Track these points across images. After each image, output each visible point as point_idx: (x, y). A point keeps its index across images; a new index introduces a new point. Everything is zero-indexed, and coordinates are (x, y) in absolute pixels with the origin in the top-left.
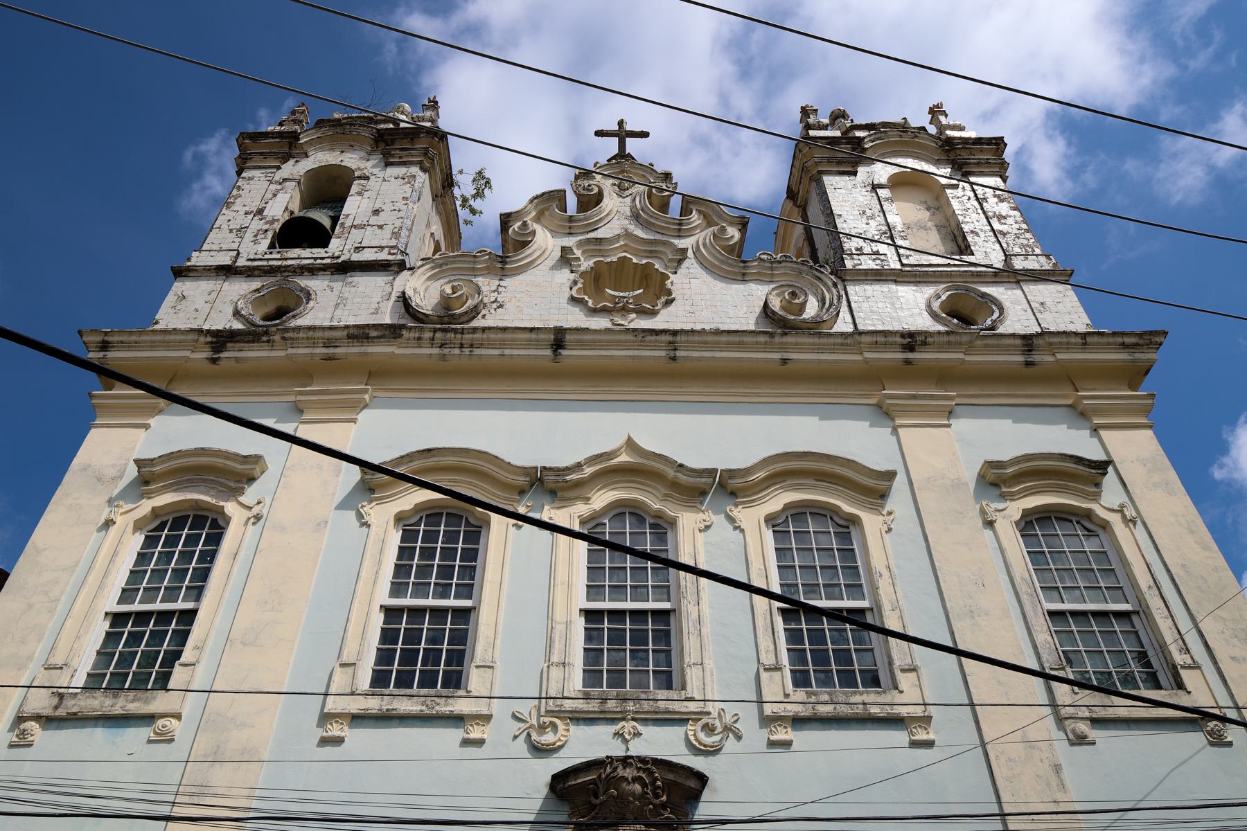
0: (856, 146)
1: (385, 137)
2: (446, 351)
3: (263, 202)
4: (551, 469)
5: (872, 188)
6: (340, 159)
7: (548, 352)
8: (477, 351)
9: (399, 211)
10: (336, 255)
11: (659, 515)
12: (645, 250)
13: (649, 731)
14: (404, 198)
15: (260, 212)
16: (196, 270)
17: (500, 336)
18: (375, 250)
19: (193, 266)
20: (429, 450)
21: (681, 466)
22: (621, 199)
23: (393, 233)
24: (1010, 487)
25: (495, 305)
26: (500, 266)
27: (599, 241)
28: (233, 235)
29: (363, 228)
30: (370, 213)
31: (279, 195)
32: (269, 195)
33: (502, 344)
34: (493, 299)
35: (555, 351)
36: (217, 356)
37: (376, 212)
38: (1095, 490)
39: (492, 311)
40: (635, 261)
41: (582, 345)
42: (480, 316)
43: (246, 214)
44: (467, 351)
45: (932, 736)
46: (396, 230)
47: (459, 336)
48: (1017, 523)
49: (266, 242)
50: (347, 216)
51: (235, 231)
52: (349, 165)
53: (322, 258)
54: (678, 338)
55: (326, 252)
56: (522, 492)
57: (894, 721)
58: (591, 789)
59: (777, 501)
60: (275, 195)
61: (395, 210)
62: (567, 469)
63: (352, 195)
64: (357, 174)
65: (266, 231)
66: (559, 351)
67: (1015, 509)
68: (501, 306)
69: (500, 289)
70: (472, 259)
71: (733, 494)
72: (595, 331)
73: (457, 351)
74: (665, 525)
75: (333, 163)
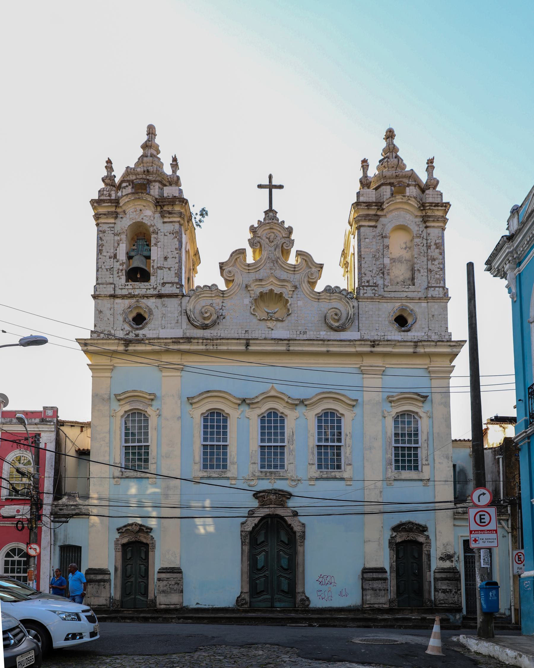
0: (379, 208)
1: (160, 204)
2: (208, 347)
3: (115, 249)
4: (248, 399)
5: (382, 237)
6: (141, 217)
7: (243, 348)
8: (219, 348)
9: (175, 258)
10: (155, 287)
11: (282, 413)
12: (280, 285)
13: (278, 482)
14: (176, 248)
15: (115, 256)
16: (101, 297)
17: (226, 341)
18: (170, 285)
19: (100, 294)
20: (208, 391)
21: (289, 397)
22: (270, 249)
23: (176, 273)
24: (395, 403)
25: (222, 317)
26: (222, 295)
27: (261, 280)
28: (108, 273)
29: (162, 269)
30: (163, 259)
31: (121, 245)
32: (116, 245)
33: (227, 344)
34: (221, 314)
35: (246, 347)
36: (126, 349)
37: (166, 258)
38: (422, 405)
39: (221, 321)
40: (275, 292)
41: (256, 344)
42: (217, 323)
43: (110, 258)
44: (215, 347)
45: (351, 484)
46: (176, 272)
47: (212, 342)
48: (393, 417)
49: (124, 278)
50: (154, 261)
51: (108, 270)
52: (146, 222)
53: (149, 289)
54: (290, 342)
55: (150, 285)
56: (239, 405)
57: (342, 479)
58: (263, 497)
59: (319, 409)
60: (118, 244)
61: (173, 257)
62: (253, 398)
63: (153, 246)
64: (151, 229)
65: (122, 270)
66: (248, 347)
67: (394, 411)
68: (224, 318)
69: (223, 308)
70: (210, 292)
71: (306, 405)
72: (260, 340)
73: (211, 347)
74: (284, 416)
75: (139, 220)
